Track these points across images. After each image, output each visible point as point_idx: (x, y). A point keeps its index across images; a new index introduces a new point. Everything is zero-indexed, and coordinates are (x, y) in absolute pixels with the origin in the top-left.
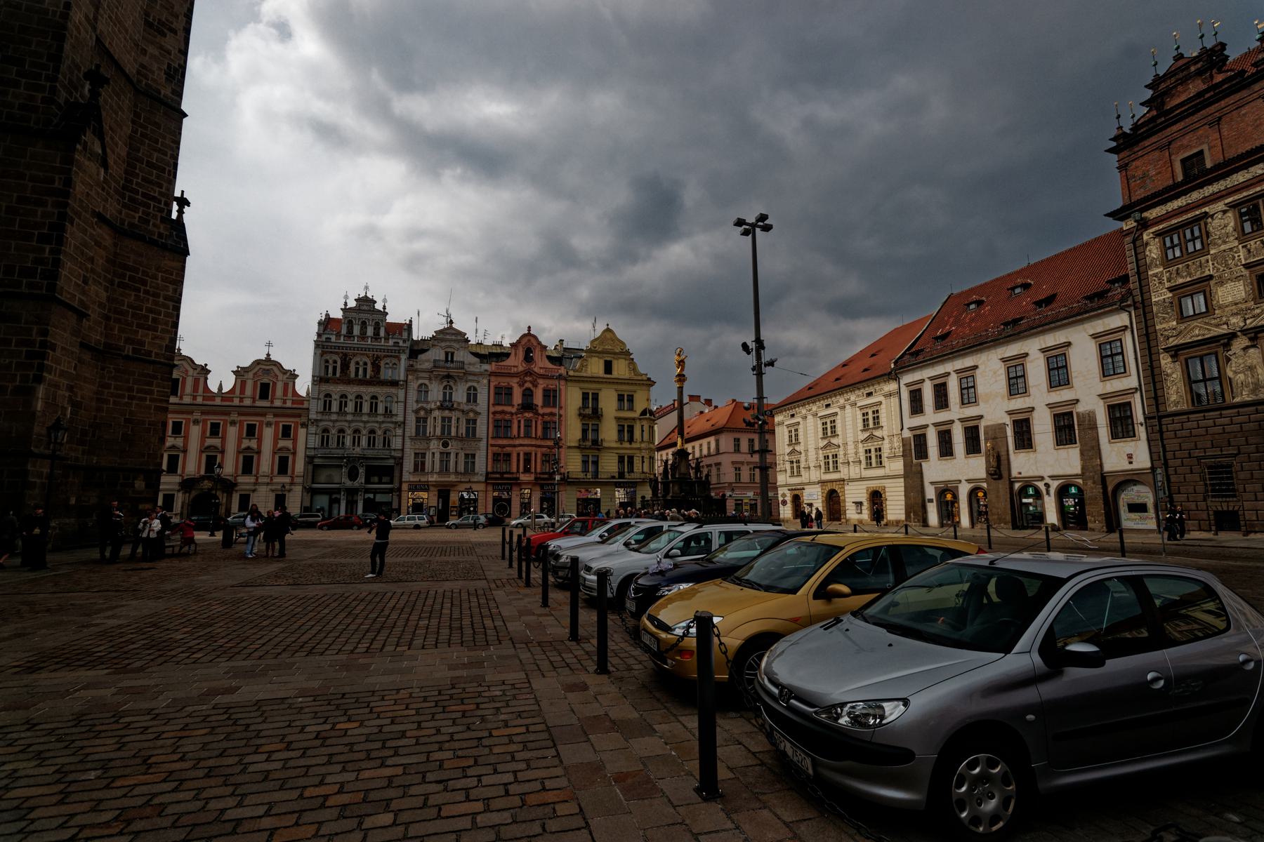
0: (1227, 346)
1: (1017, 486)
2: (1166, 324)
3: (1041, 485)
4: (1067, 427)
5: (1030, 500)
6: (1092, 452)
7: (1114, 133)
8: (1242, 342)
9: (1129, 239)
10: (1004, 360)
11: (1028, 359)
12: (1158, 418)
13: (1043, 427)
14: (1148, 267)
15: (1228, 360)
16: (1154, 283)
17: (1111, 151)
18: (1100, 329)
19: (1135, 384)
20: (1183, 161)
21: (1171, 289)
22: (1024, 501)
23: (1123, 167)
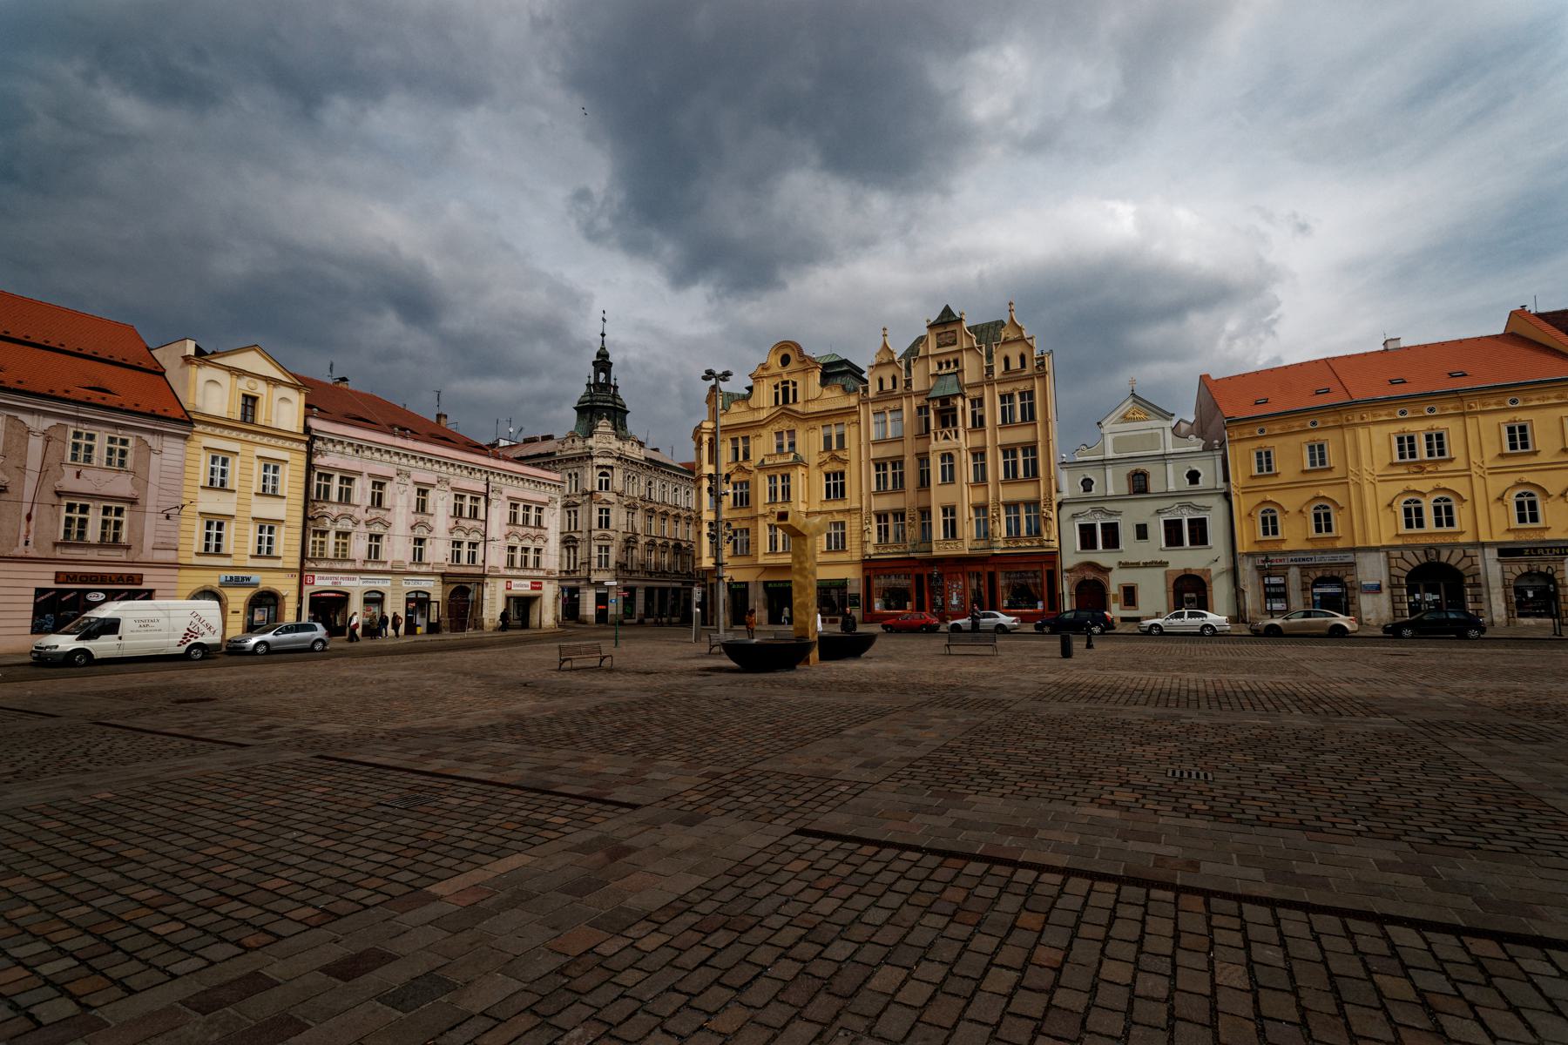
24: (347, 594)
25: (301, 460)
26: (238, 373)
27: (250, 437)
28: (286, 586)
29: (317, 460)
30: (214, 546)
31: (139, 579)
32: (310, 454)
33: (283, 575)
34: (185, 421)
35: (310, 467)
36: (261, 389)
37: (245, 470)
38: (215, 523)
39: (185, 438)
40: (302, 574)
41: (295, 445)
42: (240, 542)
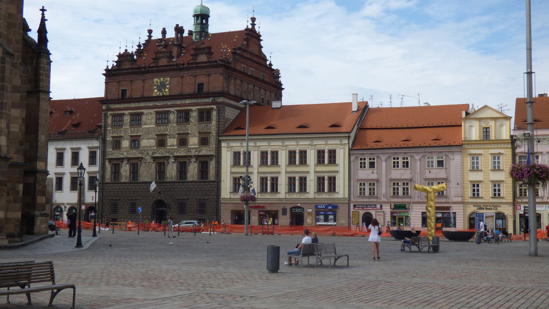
0: (122, 162)
1: (54, 207)
2: (109, 149)
3: (63, 207)
4: (76, 184)
5: (58, 213)
6: (81, 195)
7: (105, 68)
8: (126, 162)
9: (103, 113)
10: (57, 149)
11: (66, 151)
12: (103, 184)
13: (67, 182)
14: (107, 126)
15: (122, 167)
16: (108, 133)
17: (104, 74)
18: (91, 146)
19: (97, 170)
20: (122, 90)
21: (112, 137)
22: (57, 213)
23: (106, 83)
24: (540, 215)
25: (509, 152)
26: (480, 119)
27: (486, 146)
28: (507, 210)
29: (518, 150)
30: (476, 194)
31: (448, 208)
32: (514, 148)
33: (506, 206)
34: (460, 146)
35: (514, 155)
36: (492, 124)
37: (486, 162)
38: (475, 185)
39: (461, 151)
40: (514, 204)
41: (506, 146)
42: (486, 192)
